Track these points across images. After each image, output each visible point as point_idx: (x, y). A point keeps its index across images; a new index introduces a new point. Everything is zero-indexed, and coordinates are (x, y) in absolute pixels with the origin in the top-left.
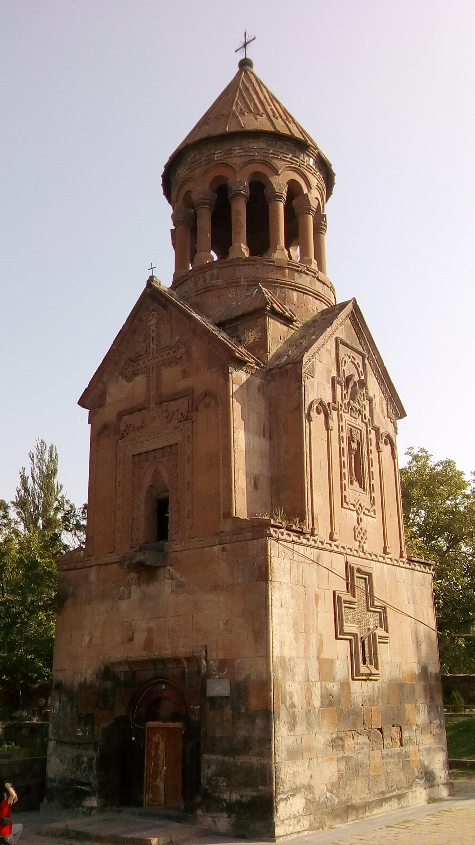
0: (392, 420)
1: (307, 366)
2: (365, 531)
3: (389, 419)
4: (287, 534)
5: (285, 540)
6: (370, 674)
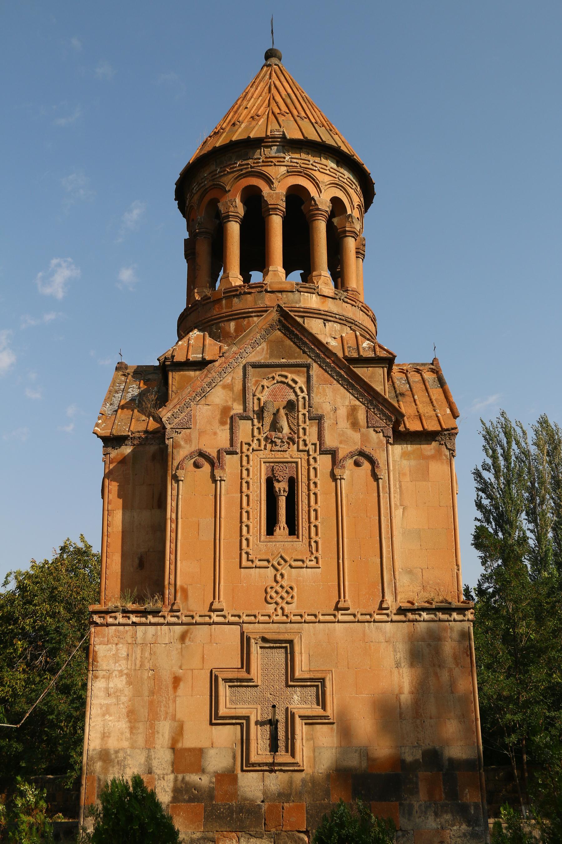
0: (376, 429)
1: (177, 420)
2: (291, 588)
3: (371, 430)
4: (123, 617)
5: (119, 624)
6: (273, 764)
